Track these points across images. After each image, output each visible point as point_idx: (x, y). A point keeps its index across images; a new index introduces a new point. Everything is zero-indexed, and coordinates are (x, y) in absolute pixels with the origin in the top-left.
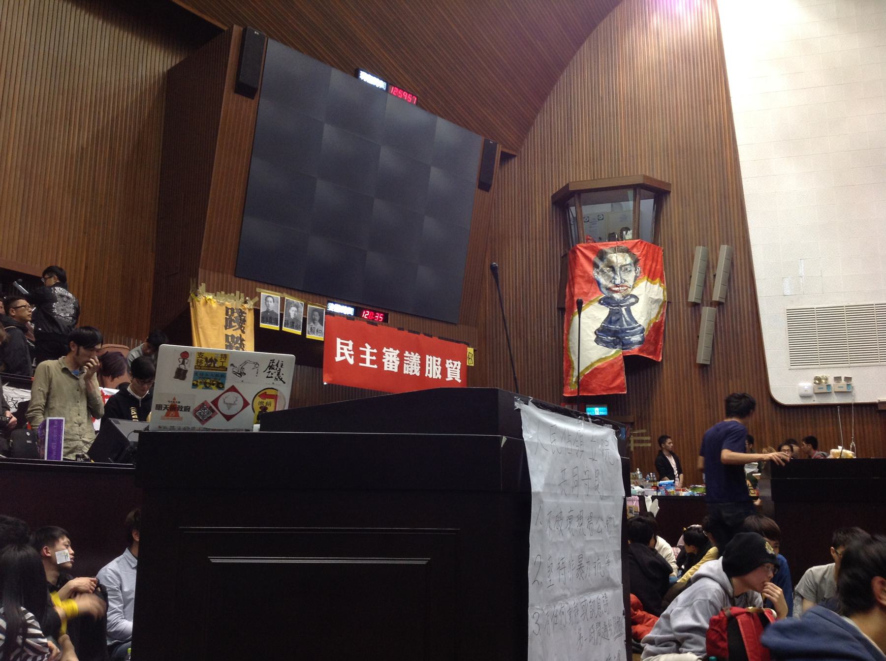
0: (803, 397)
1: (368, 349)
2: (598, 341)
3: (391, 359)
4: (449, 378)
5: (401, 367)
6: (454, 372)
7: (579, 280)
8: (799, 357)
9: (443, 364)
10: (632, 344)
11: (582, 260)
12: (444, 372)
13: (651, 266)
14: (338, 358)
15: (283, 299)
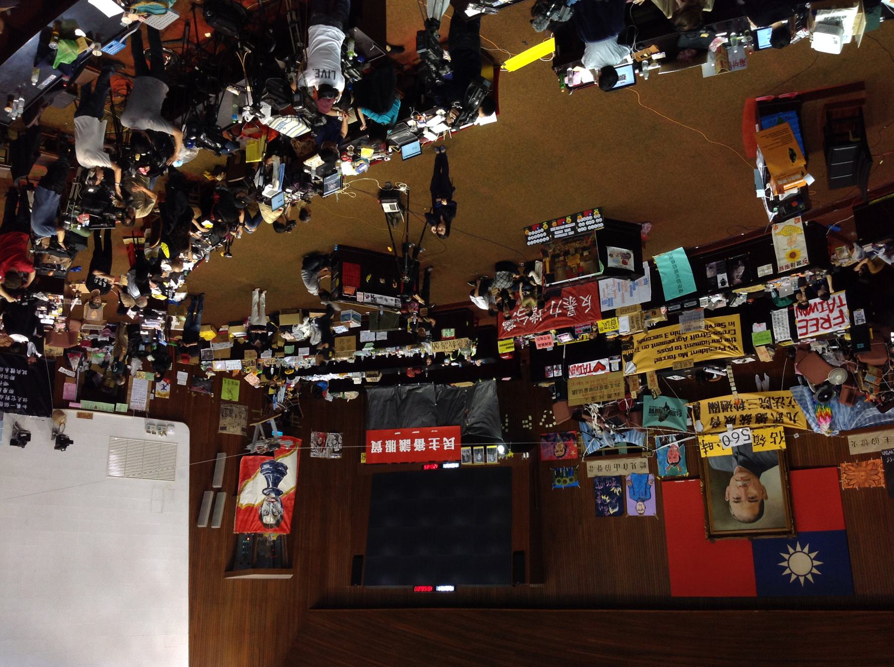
0: (173, 426)
1: (434, 448)
2: (286, 468)
3: (420, 445)
4: (380, 442)
5: (413, 442)
6: (376, 447)
7: (291, 509)
8: (174, 448)
9: (384, 449)
10: (269, 463)
11: (288, 522)
12: (383, 444)
13: (249, 515)
14: (453, 439)
15: (486, 461)
